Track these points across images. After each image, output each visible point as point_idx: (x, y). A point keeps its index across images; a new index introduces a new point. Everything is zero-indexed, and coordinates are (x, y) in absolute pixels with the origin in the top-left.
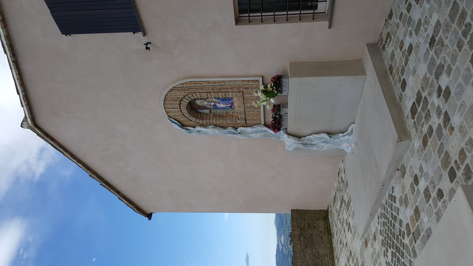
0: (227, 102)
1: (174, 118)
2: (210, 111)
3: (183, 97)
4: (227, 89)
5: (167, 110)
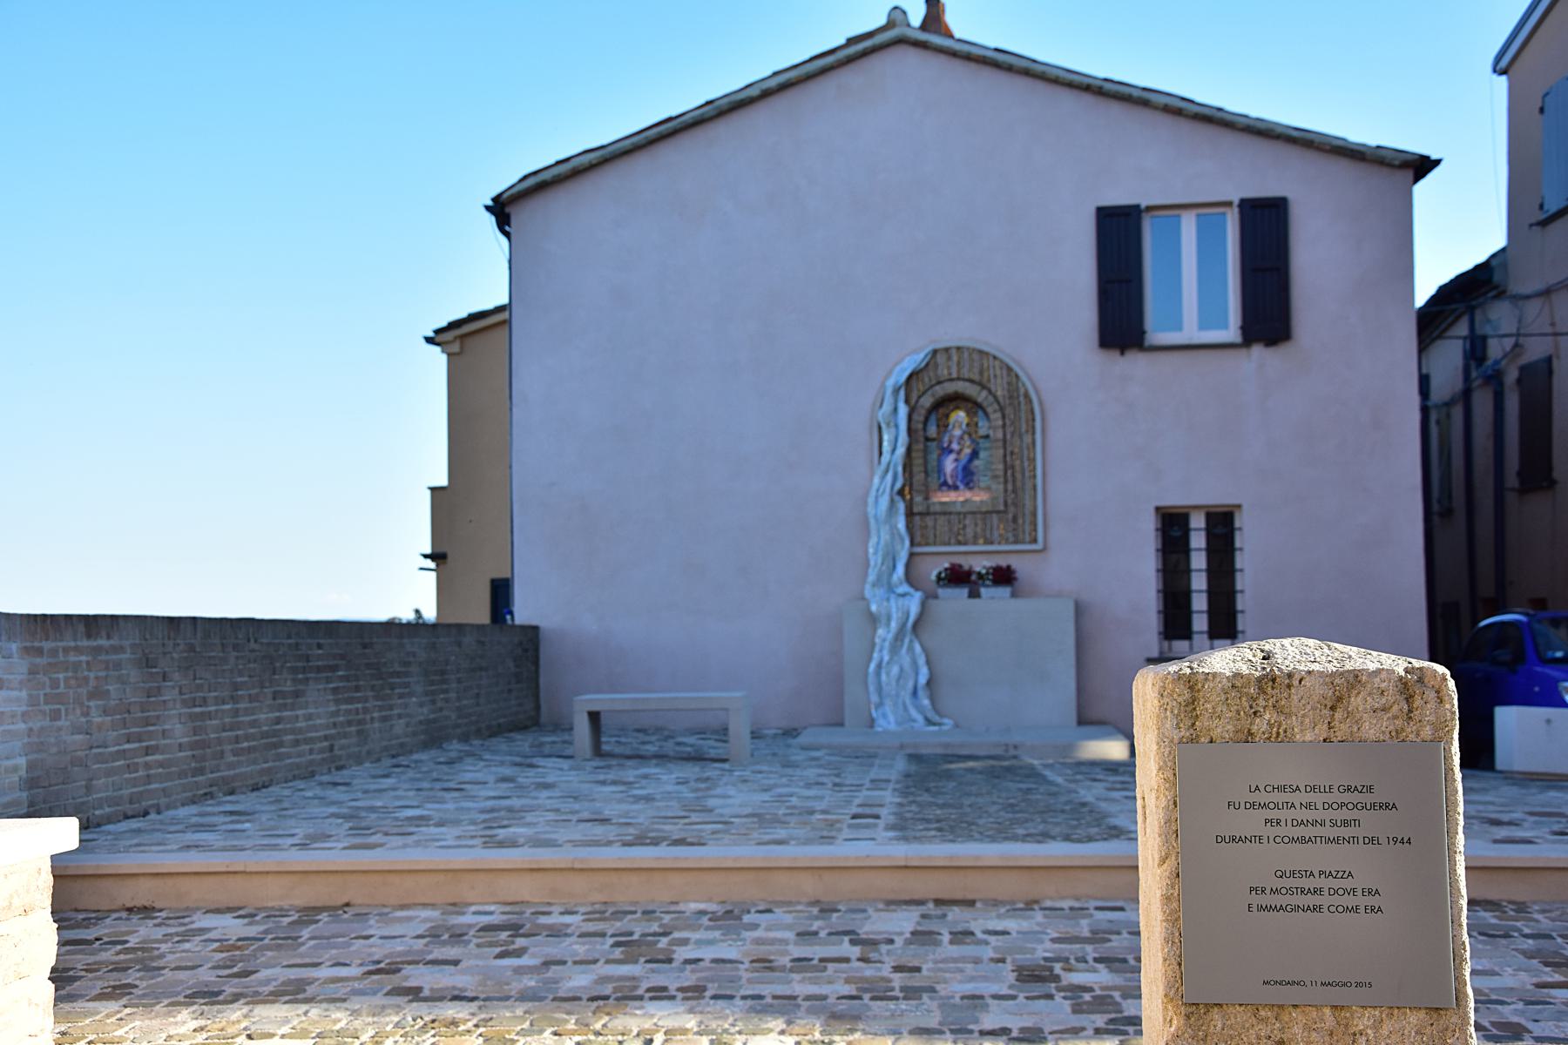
0: (960, 477)
1: (932, 362)
2: (933, 440)
3: (990, 392)
4: (1014, 481)
5: (954, 351)
